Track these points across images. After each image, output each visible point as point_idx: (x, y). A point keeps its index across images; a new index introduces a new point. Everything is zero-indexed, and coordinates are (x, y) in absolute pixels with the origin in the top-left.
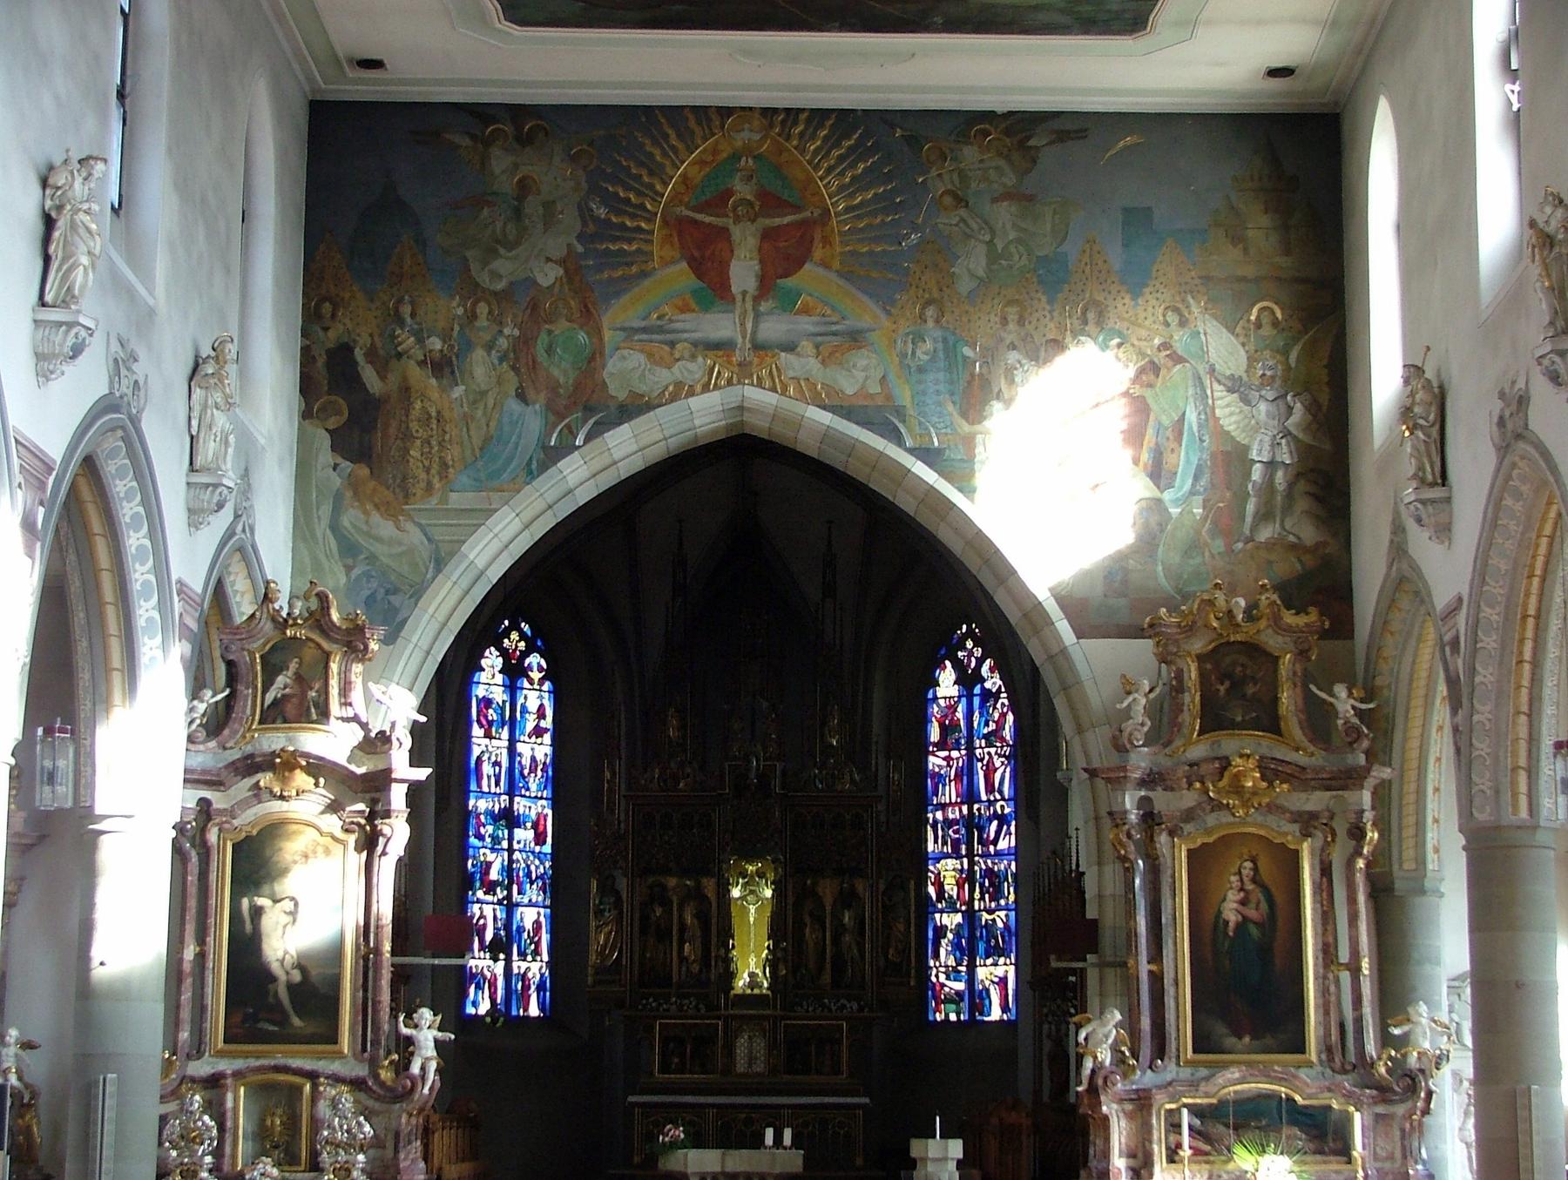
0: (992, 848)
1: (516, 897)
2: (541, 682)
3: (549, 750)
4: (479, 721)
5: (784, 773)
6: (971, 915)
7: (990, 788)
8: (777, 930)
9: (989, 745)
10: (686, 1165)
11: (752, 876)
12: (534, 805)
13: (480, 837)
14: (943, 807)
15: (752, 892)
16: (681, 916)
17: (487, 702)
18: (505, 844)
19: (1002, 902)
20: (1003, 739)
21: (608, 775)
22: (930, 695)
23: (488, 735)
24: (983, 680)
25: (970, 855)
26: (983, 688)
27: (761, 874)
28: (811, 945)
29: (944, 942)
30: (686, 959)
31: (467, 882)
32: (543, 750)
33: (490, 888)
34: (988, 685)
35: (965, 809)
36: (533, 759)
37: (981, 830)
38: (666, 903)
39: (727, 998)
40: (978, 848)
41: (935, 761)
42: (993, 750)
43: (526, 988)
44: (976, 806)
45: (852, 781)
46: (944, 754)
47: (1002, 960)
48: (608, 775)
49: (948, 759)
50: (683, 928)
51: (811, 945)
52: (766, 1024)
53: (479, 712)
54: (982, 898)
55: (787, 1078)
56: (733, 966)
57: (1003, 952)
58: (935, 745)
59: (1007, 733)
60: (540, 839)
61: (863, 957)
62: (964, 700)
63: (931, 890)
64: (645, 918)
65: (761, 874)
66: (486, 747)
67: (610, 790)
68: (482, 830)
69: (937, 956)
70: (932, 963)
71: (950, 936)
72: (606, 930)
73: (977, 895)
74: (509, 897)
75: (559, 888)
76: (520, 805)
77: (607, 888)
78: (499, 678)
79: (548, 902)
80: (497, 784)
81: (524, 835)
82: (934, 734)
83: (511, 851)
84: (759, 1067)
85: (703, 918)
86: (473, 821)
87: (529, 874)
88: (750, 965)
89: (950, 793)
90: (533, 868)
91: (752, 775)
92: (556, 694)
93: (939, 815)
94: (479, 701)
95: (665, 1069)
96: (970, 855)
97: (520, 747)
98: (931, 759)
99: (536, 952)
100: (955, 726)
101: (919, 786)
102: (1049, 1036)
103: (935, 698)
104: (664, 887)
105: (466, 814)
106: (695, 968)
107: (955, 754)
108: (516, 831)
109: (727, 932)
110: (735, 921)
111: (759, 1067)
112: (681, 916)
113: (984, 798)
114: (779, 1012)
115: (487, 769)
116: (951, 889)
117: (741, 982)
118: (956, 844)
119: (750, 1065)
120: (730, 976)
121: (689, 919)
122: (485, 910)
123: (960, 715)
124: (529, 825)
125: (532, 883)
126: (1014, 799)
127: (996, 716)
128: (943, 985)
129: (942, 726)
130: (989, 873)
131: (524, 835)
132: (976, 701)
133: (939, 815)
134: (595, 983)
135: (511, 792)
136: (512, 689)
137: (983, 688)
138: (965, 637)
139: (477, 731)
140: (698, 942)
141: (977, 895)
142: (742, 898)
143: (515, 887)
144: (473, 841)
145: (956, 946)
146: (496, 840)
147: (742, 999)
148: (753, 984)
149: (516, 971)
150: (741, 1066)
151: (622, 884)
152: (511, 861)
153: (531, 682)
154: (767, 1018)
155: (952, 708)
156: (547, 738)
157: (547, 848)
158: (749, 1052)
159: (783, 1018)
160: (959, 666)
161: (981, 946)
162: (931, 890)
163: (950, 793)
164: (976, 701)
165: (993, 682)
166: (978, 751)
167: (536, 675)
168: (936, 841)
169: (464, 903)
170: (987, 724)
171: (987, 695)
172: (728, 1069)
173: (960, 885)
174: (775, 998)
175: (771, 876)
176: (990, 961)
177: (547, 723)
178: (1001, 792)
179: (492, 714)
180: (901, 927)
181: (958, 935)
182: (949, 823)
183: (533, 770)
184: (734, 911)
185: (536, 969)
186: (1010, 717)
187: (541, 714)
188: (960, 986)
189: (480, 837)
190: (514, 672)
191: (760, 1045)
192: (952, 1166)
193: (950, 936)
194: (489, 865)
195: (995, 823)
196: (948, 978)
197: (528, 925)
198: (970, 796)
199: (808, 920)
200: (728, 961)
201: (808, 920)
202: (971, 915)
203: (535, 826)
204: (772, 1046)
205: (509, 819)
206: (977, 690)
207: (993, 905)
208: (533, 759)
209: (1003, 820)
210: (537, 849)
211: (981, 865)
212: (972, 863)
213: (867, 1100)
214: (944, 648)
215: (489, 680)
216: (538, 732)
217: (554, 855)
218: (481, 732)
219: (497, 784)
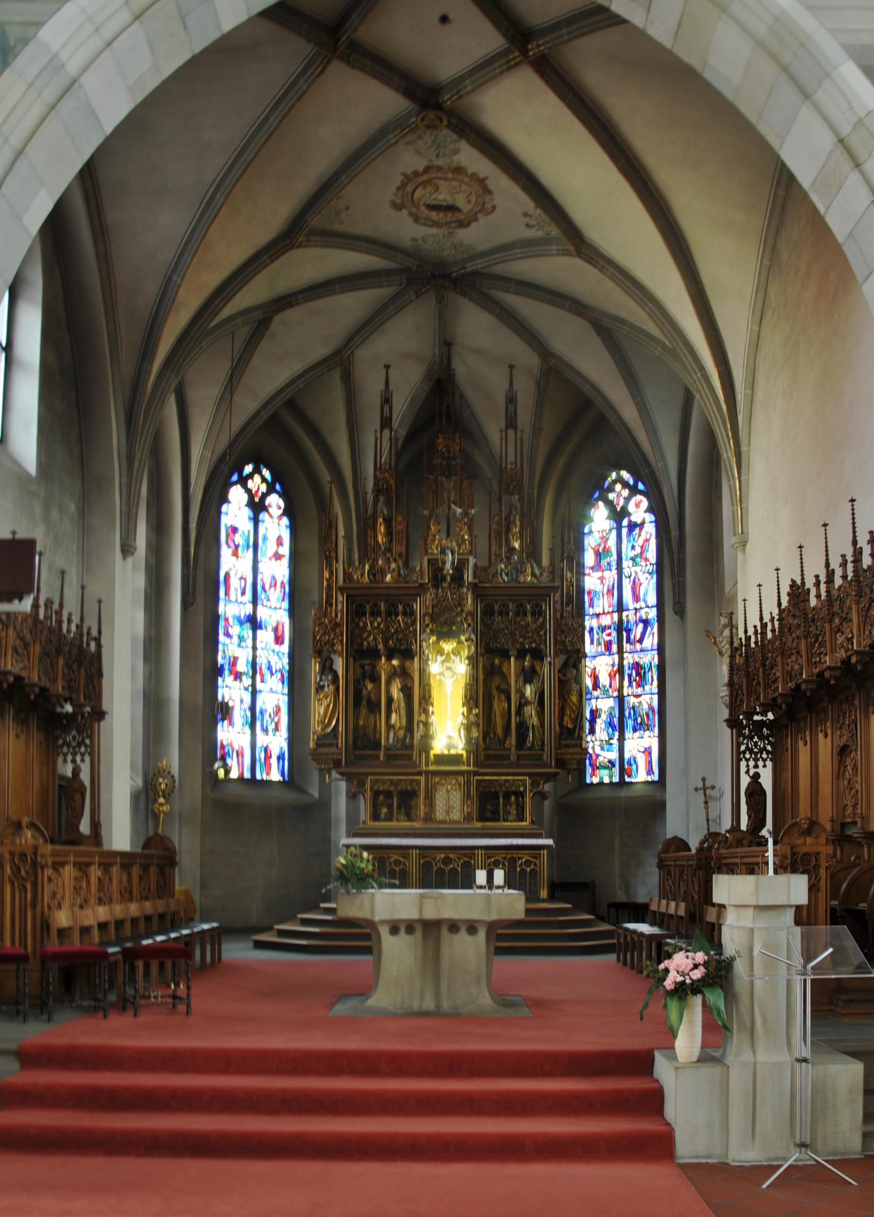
0: (638, 646)
1: (259, 686)
2: (280, 518)
3: (286, 572)
4: (227, 543)
5: (475, 566)
6: (621, 699)
7: (636, 598)
8: (471, 700)
9: (635, 564)
10: (372, 911)
11: (448, 654)
12: (275, 612)
13: (227, 635)
14: (598, 616)
15: (448, 668)
16: (388, 691)
17: (235, 530)
18: (250, 642)
19: (647, 688)
20: (647, 560)
21: (326, 575)
22: (586, 530)
23: (235, 554)
24: (629, 515)
25: (621, 652)
26: (630, 521)
27: (456, 652)
28: (498, 713)
29: (598, 721)
30: (393, 726)
31: (220, 671)
32: (281, 570)
33: (238, 676)
34: (634, 518)
35: (616, 615)
36: (274, 578)
37: (629, 631)
38: (375, 678)
39: (427, 757)
40: (627, 647)
41: (591, 582)
42: (638, 569)
43: (268, 757)
44: (625, 614)
45: (533, 575)
46: (599, 574)
47: (647, 733)
48: (326, 575)
49: (602, 579)
50: (390, 700)
51: (498, 713)
52: (461, 779)
53: (228, 535)
54: (630, 685)
55: (479, 825)
56: (432, 729)
57: (649, 728)
58: (592, 568)
59: (652, 554)
60: (279, 640)
61: (542, 724)
62: (614, 532)
63: (589, 682)
64: (358, 693)
65: (456, 652)
66: (233, 565)
67: (329, 587)
68: (231, 631)
69: (592, 731)
70: (589, 738)
71: (604, 716)
72: (325, 703)
73: (626, 683)
74: (254, 685)
75: (295, 679)
76: (262, 613)
77: (327, 668)
78: (247, 512)
79: (286, 691)
80: (243, 593)
81: (265, 636)
82: (589, 559)
83: (254, 648)
84: (456, 815)
85: (407, 691)
86: (222, 623)
87: (270, 668)
88: (448, 728)
89: (603, 604)
90: (273, 664)
91: (448, 566)
92: (294, 529)
93: (594, 623)
94: (227, 528)
95: (376, 817)
96: (621, 652)
97: (261, 567)
98: (587, 578)
99: (277, 729)
100: (607, 550)
101: (575, 603)
102: (747, 772)
103: (590, 532)
104: (374, 667)
105: (216, 618)
106: (401, 733)
107: (607, 574)
108: (259, 632)
109: (426, 699)
110: (435, 693)
111: (456, 815)
112: (388, 691)
113: (631, 606)
114: (472, 768)
115: (234, 583)
116: (604, 680)
117: (439, 746)
118: (608, 645)
119: (448, 813)
120: (427, 737)
121: (396, 693)
122: (231, 691)
123: (612, 543)
124: (270, 628)
125: (272, 674)
126: (660, 606)
127: (641, 541)
128: (598, 756)
129: (598, 555)
130: (637, 666)
131: (265, 636)
132: (625, 531)
133: (594, 623)
134: (318, 745)
135: (255, 601)
136: (256, 521)
137: (630, 521)
138: (614, 482)
139: (226, 552)
140: (403, 712)
141: (626, 683)
142: (442, 674)
143: (258, 677)
144: (222, 638)
145: (610, 724)
146: (241, 639)
147: (441, 759)
148: (450, 747)
149: (259, 744)
150: (440, 814)
151: (339, 665)
152: (254, 657)
153: (271, 516)
154: (461, 773)
155: (605, 539)
156: (285, 561)
157: (285, 648)
158: (450, 802)
159: (476, 773)
160: (610, 504)
161: (630, 723)
162: (589, 682)
163: (603, 604)
164: (625, 531)
165: (639, 510)
166: (626, 571)
167: (275, 512)
168: (592, 643)
169: (215, 688)
170: (633, 548)
171: (632, 526)
172: (429, 817)
173: (611, 676)
174: (468, 758)
175: (465, 653)
176: (637, 734)
177: (285, 550)
178: (645, 601)
179: (238, 539)
180: (574, 699)
181: (610, 715)
182: (604, 629)
183: (274, 584)
184: (433, 683)
185: (277, 742)
186: (653, 542)
187: (279, 542)
188: (614, 755)
189: (227, 635)
190: (257, 507)
191: (456, 797)
192: (790, 914)
193: (604, 716)
194: (236, 659)
195: (641, 626)
196: (602, 748)
197: (270, 709)
198: (620, 607)
199: (495, 693)
200: (427, 725)
201: (495, 693)
202: (621, 699)
203: (276, 629)
204: (467, 796)
205: (254, 622)
206: (625, 522)
207: (639, 691)
208: (274, 578)
209: (646, 623)
210: (277, 648)
211: (629, 659)
212: (621, 659)
213: (550, 842)
214: (596, 489)
215: (235, 510)
216: (278, 556)
217: (292, 656)
218: (230, 551)
219: (243, 593)
